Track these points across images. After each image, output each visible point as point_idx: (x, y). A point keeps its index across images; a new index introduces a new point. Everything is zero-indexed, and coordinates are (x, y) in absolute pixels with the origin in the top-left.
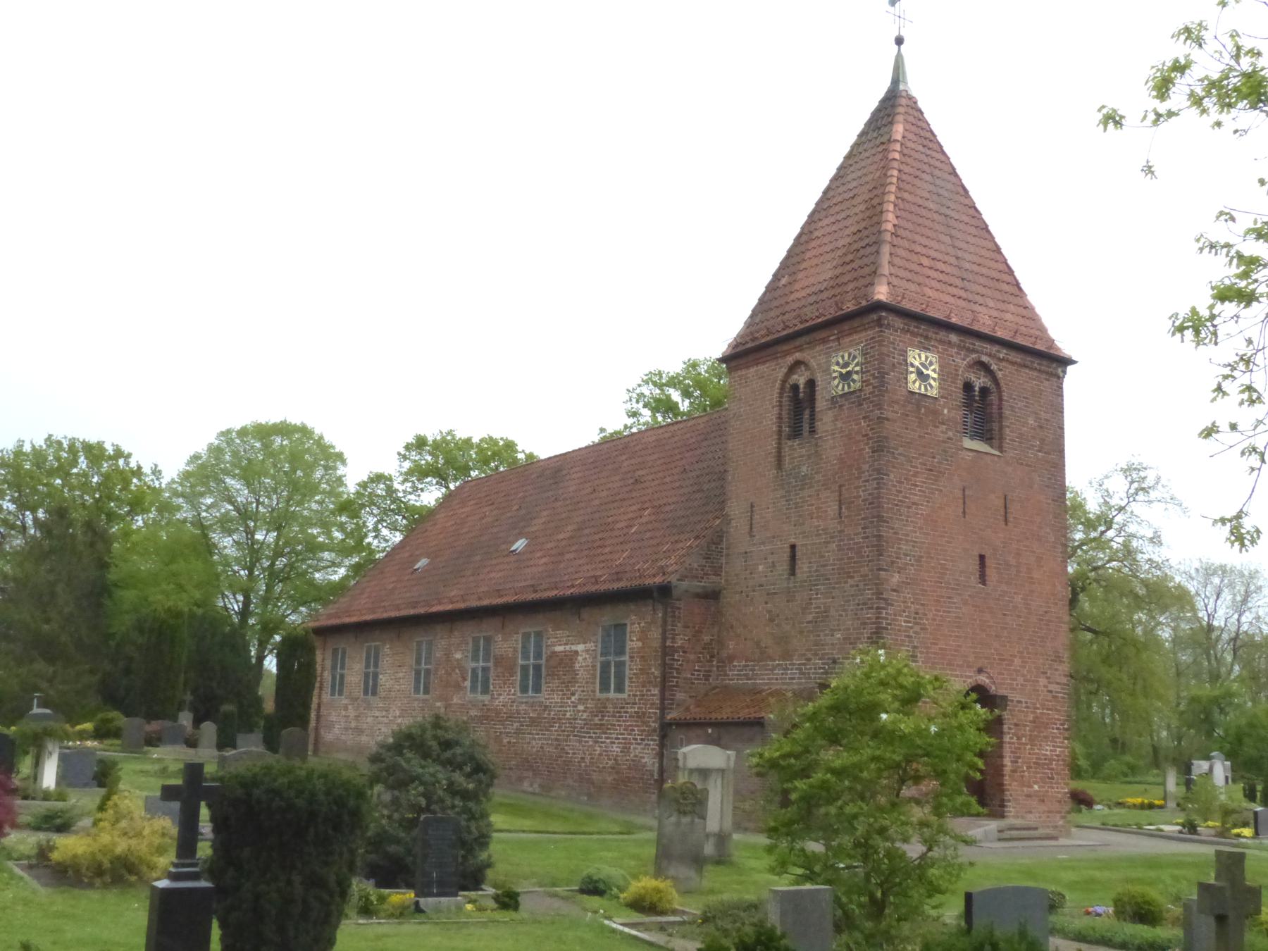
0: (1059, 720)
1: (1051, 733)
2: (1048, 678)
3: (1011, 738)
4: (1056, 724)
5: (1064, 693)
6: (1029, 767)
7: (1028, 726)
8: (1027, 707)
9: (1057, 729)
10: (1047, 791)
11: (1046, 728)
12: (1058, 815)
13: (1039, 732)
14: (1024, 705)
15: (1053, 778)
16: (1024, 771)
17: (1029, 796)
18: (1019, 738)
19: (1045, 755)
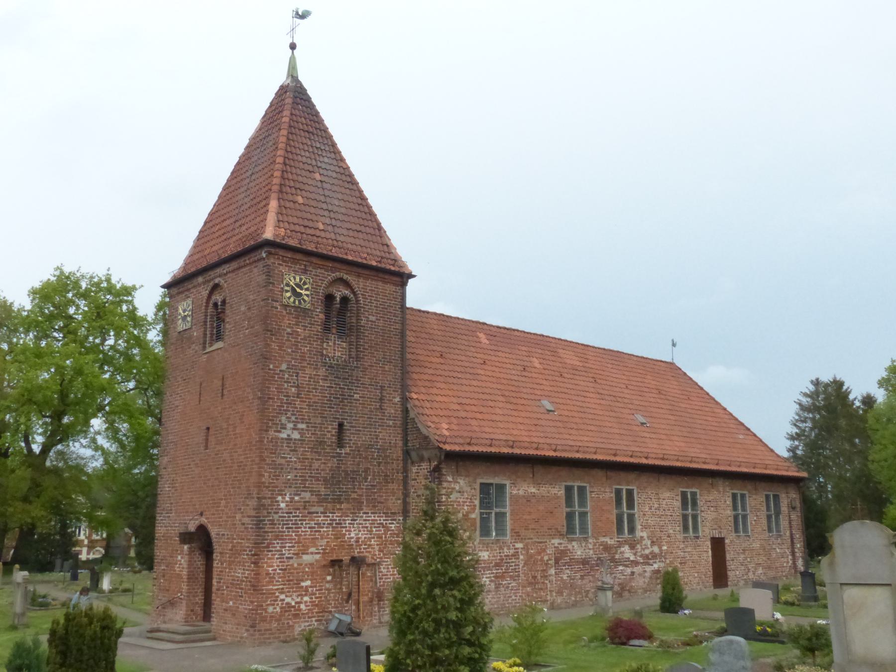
0: (248, 547)
1: (243, 558)
2: (242, 513)
3: (217, 564)
4: (246, 551)
5: (253, 524)
6: (227, 587)
7: (227, 553)
8: (228, 539)
9: (247, 555)
10: (238, 607)
11: (239, 554)
12: (244, 628)
13: (235, 558)
14: (226, 537)
15: (242, 596)
16: (224, 590)
17: (226, 610)
18: (222, 564)
19: (238, 577)
